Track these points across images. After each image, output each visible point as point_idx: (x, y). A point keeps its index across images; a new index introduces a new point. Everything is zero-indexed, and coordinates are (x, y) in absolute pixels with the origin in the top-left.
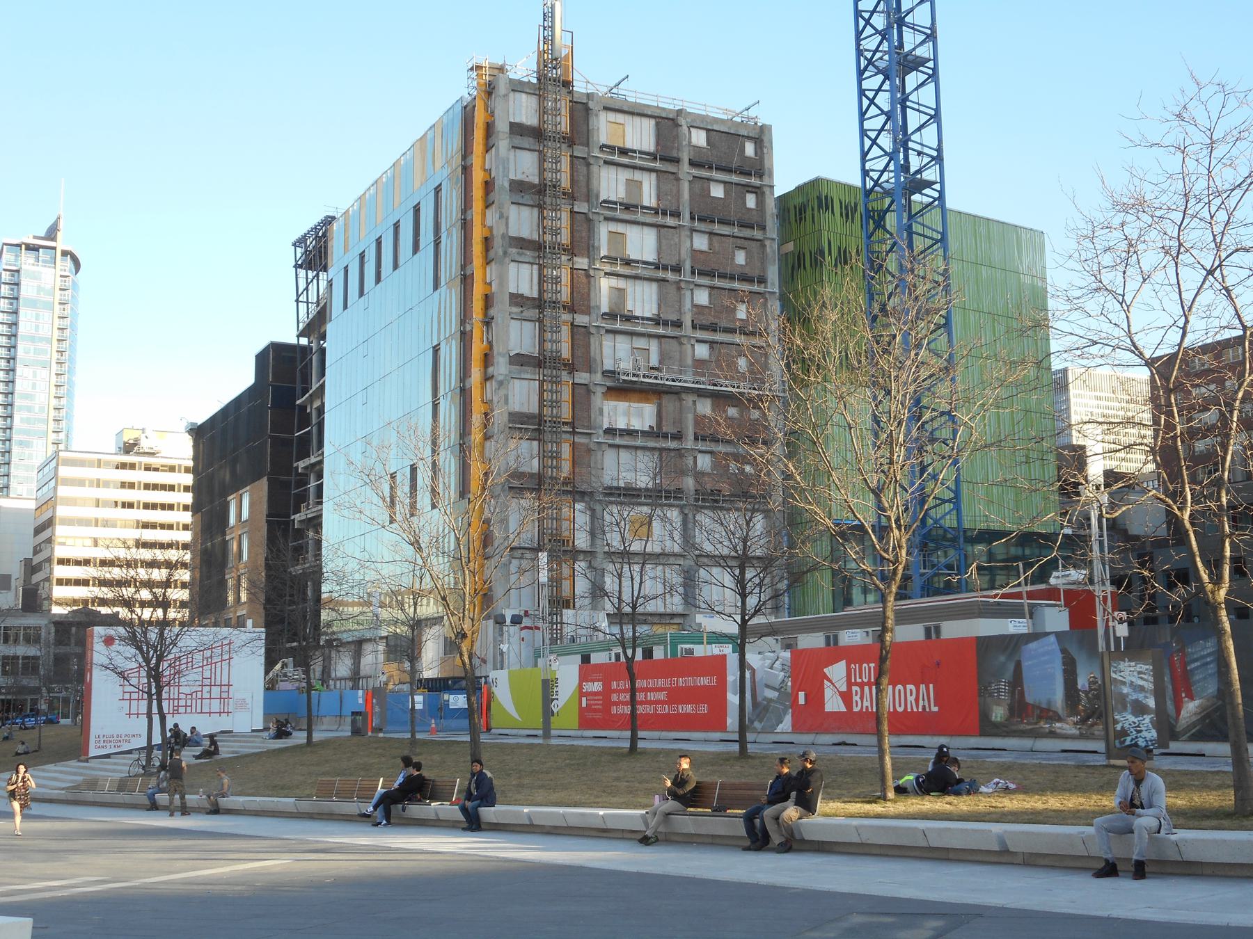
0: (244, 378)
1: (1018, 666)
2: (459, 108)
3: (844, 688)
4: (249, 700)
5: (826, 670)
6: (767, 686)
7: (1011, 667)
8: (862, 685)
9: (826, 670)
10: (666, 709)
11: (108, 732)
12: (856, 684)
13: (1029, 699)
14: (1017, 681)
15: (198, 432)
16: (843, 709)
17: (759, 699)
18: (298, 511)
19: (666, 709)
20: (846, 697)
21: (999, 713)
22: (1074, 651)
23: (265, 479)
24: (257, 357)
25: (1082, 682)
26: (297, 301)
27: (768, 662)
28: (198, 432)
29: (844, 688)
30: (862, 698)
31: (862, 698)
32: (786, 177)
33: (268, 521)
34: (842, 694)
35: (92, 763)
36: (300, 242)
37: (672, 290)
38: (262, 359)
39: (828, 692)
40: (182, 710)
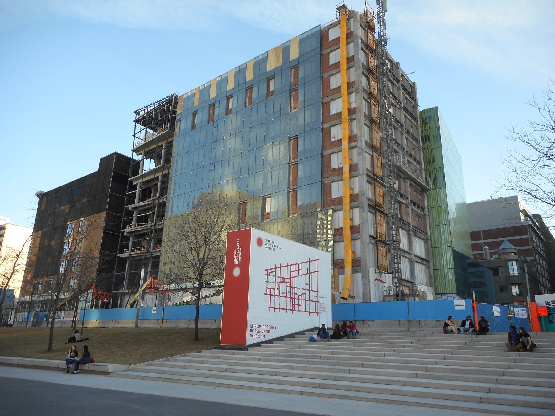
0: (95, 168)
2: (318, 29)
4: (326, 304)
11: (257, 322)
15: (42, 196)
18: (125, 228)
23: (105, 212)
24: (101, 160)
26: (134, 136)
28: (42, 196)
32: (423, 105)
33: (104, 232)
35: (250, 350)
36: (136, 112)
37: (399, 134)
38: (104, 162)
40: (296, 307)
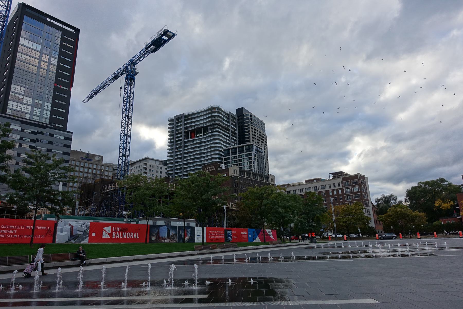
1: (159, 230)
3: (110, 232)
5: (104, 228)
6: (78, 231)
7: (157, 231)
8: (116, 232)
9: (104, 228)
10: (16, 236)
12: (114, 232)
13: (160, 236)
14: (158, 233)
16: (109, 237)
17: (74, 234)
19: (16, 236)
20: (111, 235)
21: (154, 238)
22: (170, 229)
25: (171, 234)
27: (79, 225)
29: (110, 232)
30: (116, 235)
31: (116, 235)
34: (109, 234)
39: (104, 233)
